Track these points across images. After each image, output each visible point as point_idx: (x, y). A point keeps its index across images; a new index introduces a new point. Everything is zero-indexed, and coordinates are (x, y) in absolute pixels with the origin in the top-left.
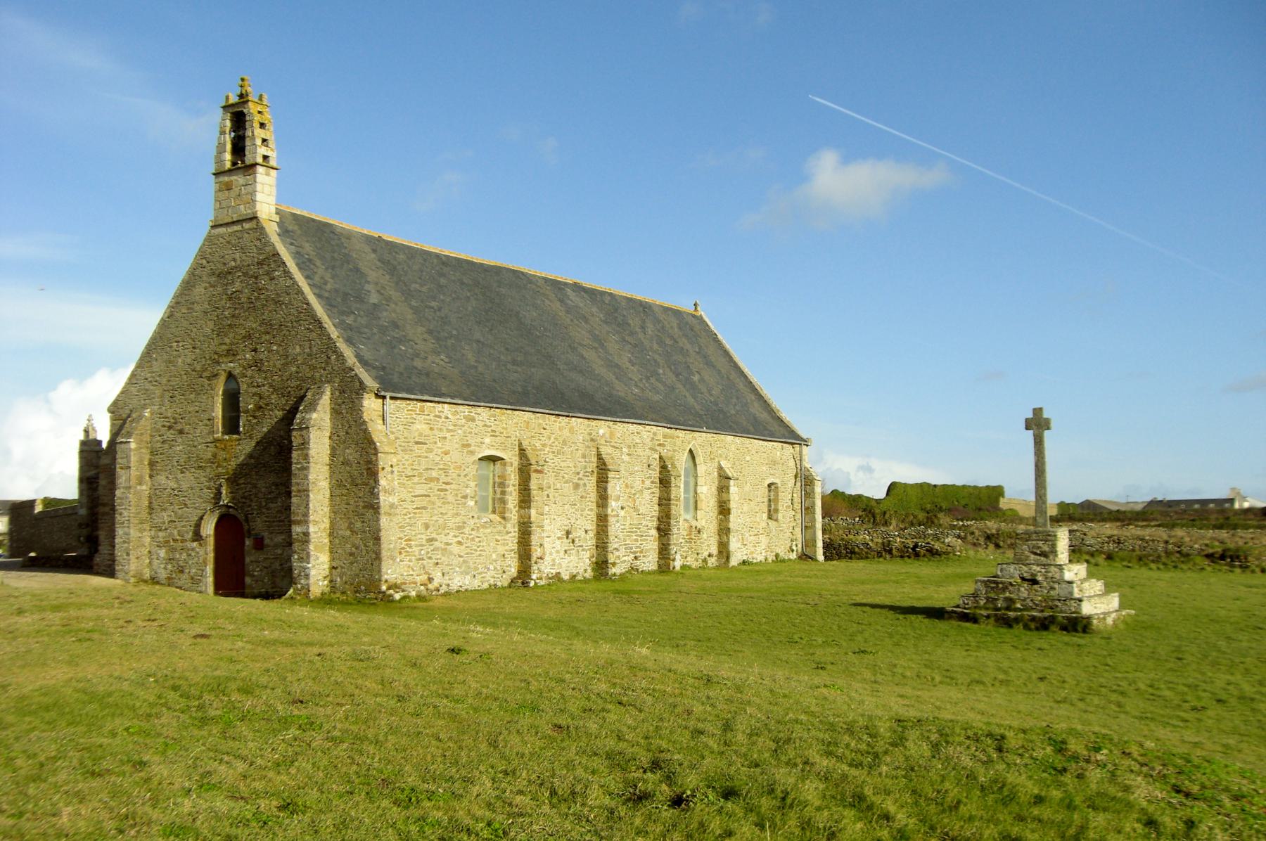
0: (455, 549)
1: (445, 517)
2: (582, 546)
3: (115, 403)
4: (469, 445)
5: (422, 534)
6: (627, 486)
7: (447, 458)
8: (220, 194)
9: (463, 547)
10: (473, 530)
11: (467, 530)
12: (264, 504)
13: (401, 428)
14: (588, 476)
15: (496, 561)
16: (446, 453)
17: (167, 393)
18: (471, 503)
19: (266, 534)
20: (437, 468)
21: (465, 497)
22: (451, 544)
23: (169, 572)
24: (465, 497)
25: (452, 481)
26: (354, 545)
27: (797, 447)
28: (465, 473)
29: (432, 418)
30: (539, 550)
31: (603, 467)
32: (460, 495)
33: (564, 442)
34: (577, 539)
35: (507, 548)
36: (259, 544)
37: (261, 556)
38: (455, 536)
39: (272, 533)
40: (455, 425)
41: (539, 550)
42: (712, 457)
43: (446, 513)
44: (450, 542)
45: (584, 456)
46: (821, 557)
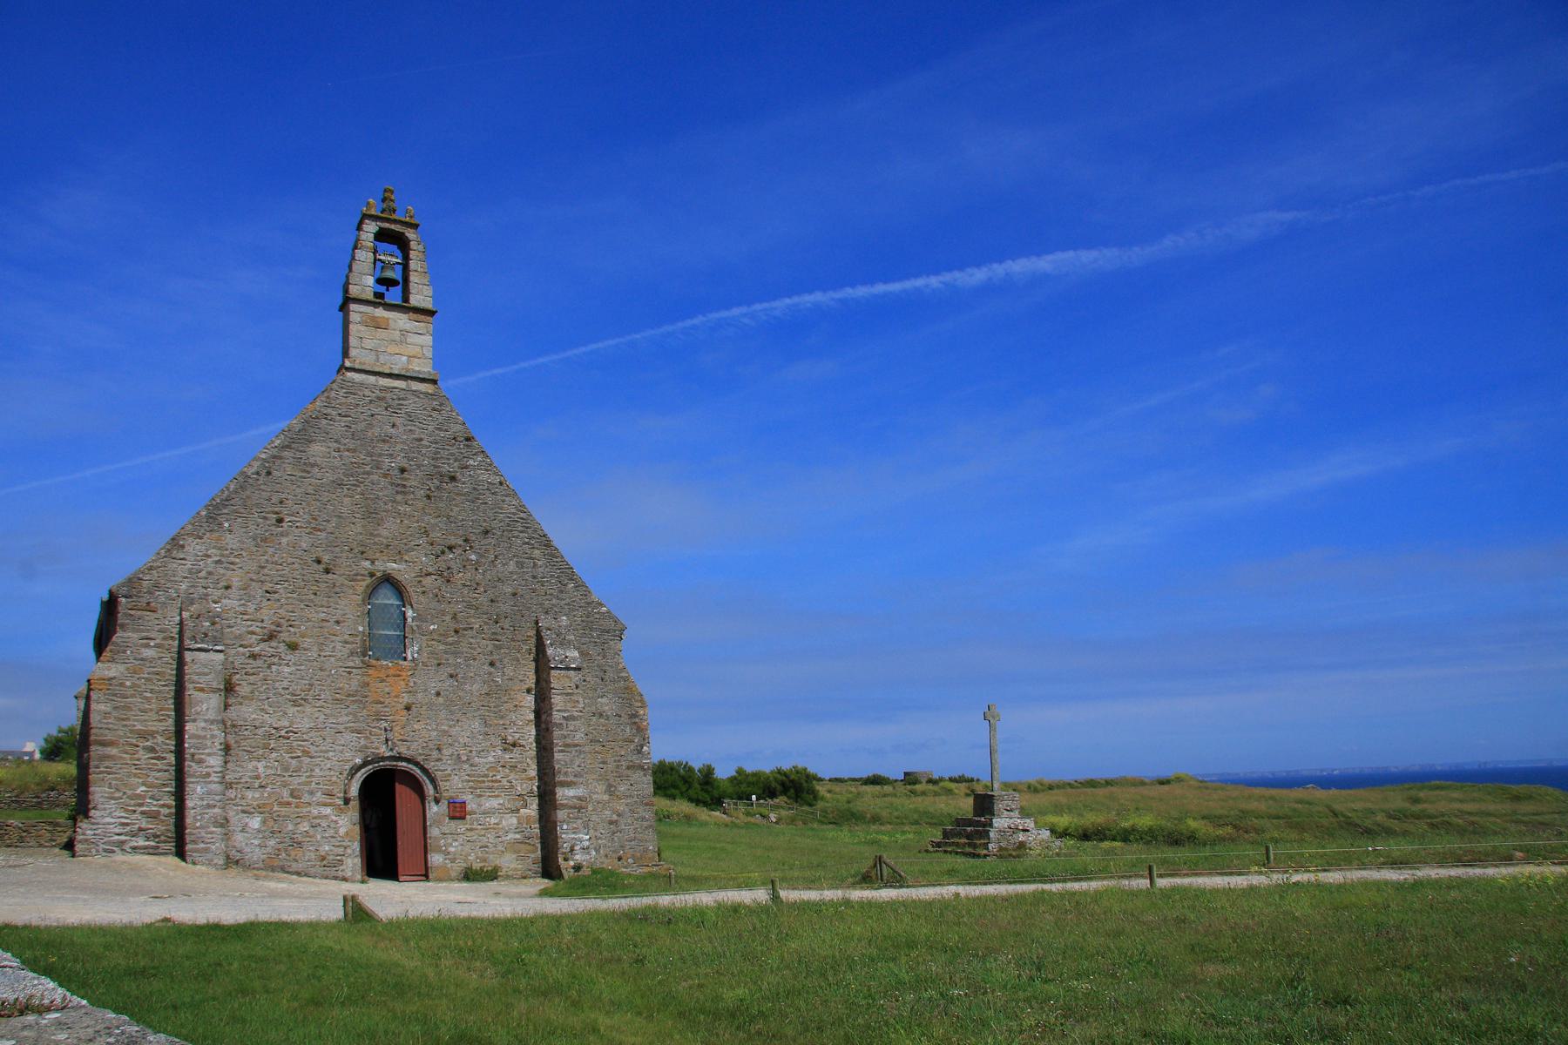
19: (467, 797)
23: (269, 850)
36: (458, 811)
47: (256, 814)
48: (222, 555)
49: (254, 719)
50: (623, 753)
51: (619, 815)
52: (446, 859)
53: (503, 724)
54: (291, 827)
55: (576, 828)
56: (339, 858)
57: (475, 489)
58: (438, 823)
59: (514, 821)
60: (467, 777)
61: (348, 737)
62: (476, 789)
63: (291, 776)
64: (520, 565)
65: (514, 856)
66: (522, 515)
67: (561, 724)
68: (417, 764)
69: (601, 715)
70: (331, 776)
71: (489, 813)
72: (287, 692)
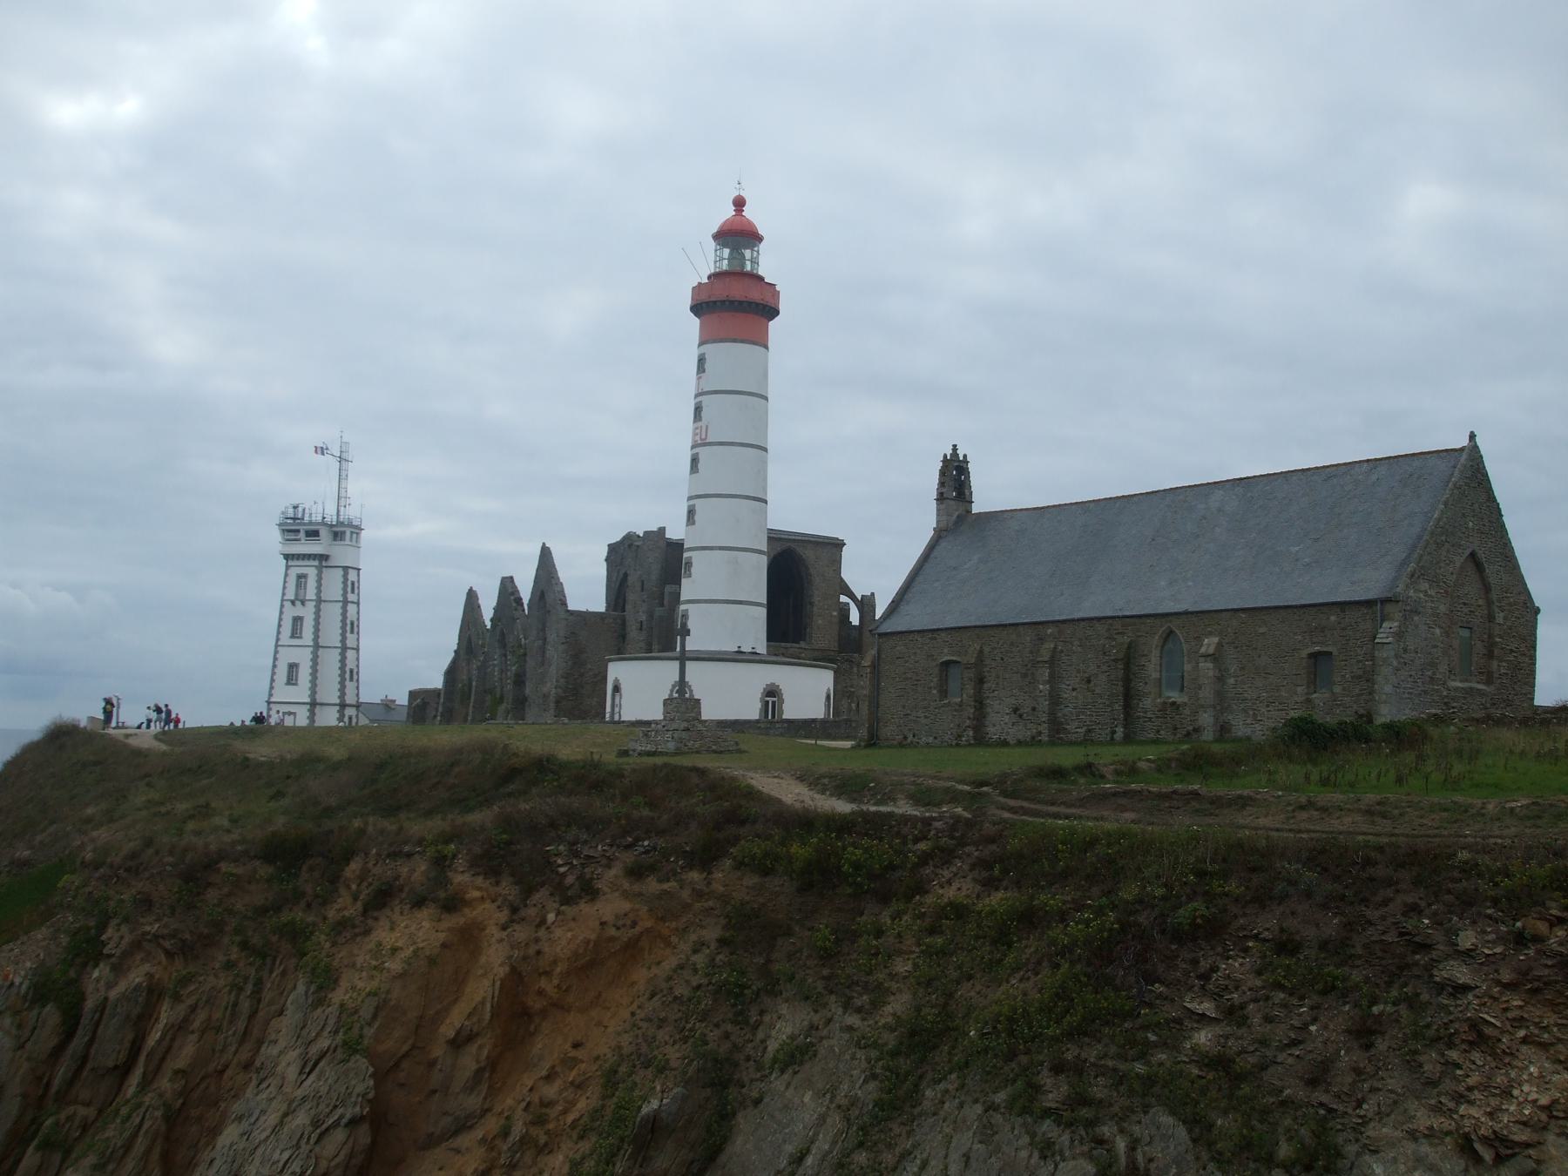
6: (1078, 671)
7: (917, 665)
18: (935, 692)
21: (931, 688)
33: (1012, 644)
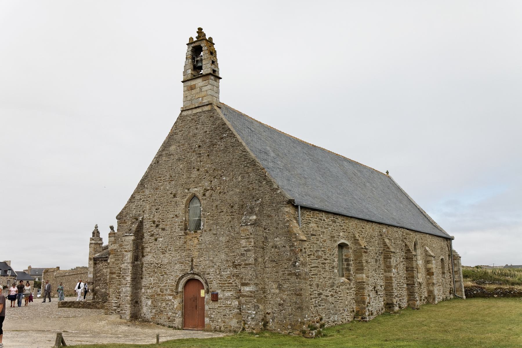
0: (330, 299)
1: (326, 279)
2: (380, 295)
3: (121, 214)
4: (333, 237)
5: (316, 290)
7: (325, 244)
8: (187, 92)
9: (333, 298)
10: (337, 287)
11: (335, 288)
12: (218, 273)
13: (304, 225)
14: (380, 255)
15: (347, 305)
16: (325, 241)
17: (153, 207)
18: (336, 271)
19: (219, 291)
20: (321, 250)
22: (328, 296)
23: (153, 314)
24: (333, 268)
25: (327, 258)
26: (281, 299)
27: (449, 241)
28: (333, 253)
29: (318, 220)
30: (368, 298)
31: (388, 250)
32: (331, 266)
34: (378, 291)
35: (351, 297)
36: (215, 298)
37: (216, 305)
38: (330, 291)
39: (224, 291)
40: (328, 225)
41: (368, 298)
42: (423, 245)
43: (326, 277)
44: (328, 294)
45: (378, 244)
46: (464, 297)
47: (150, 299)
48: (144, 198)
49: (151, 261)
50: (286, 267)
51: (284, 301)
52: (210, 321)
53: (234, 255)
54: (160, 305)
55: (249, 308)
56: (174, 318)
57: (226, 147)
58: (208, 303)
59: (237, 303)
60: (219, 282)
61: (178, 266)
62: (222, 287)
63: (161, 283)
64: (243, 177)
65: (237, 320)
66: (244, 153)
67: (244, 254)
68: (200, 276)
69: (276, 247)
70: (172, 283)
71: (227, 299)
72: (161, 248)
